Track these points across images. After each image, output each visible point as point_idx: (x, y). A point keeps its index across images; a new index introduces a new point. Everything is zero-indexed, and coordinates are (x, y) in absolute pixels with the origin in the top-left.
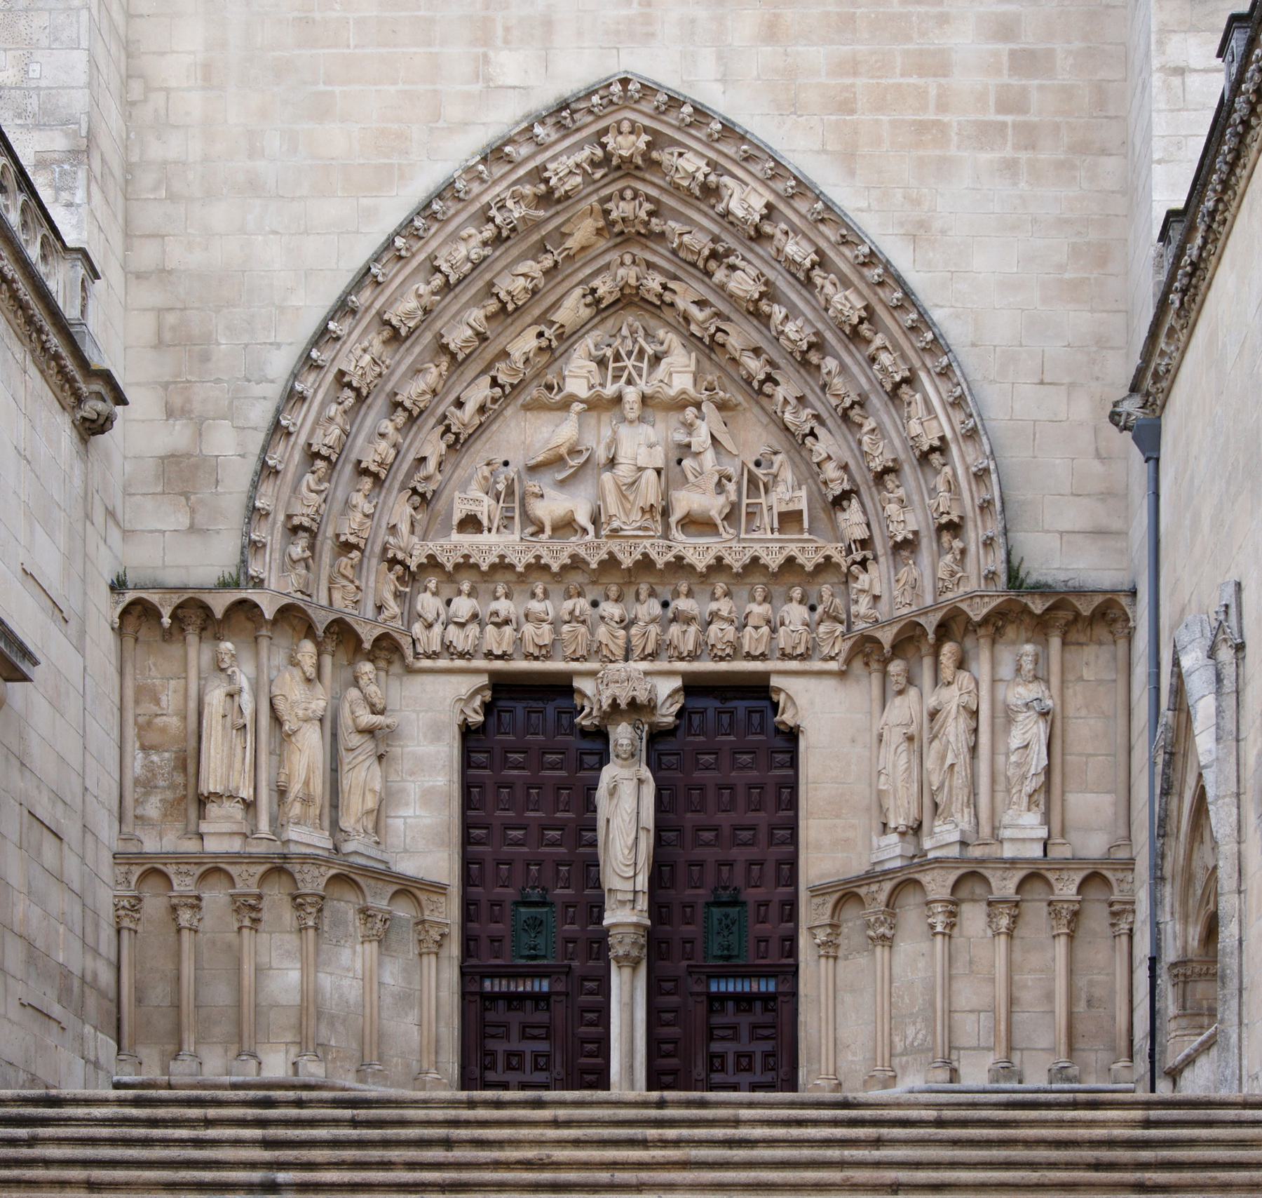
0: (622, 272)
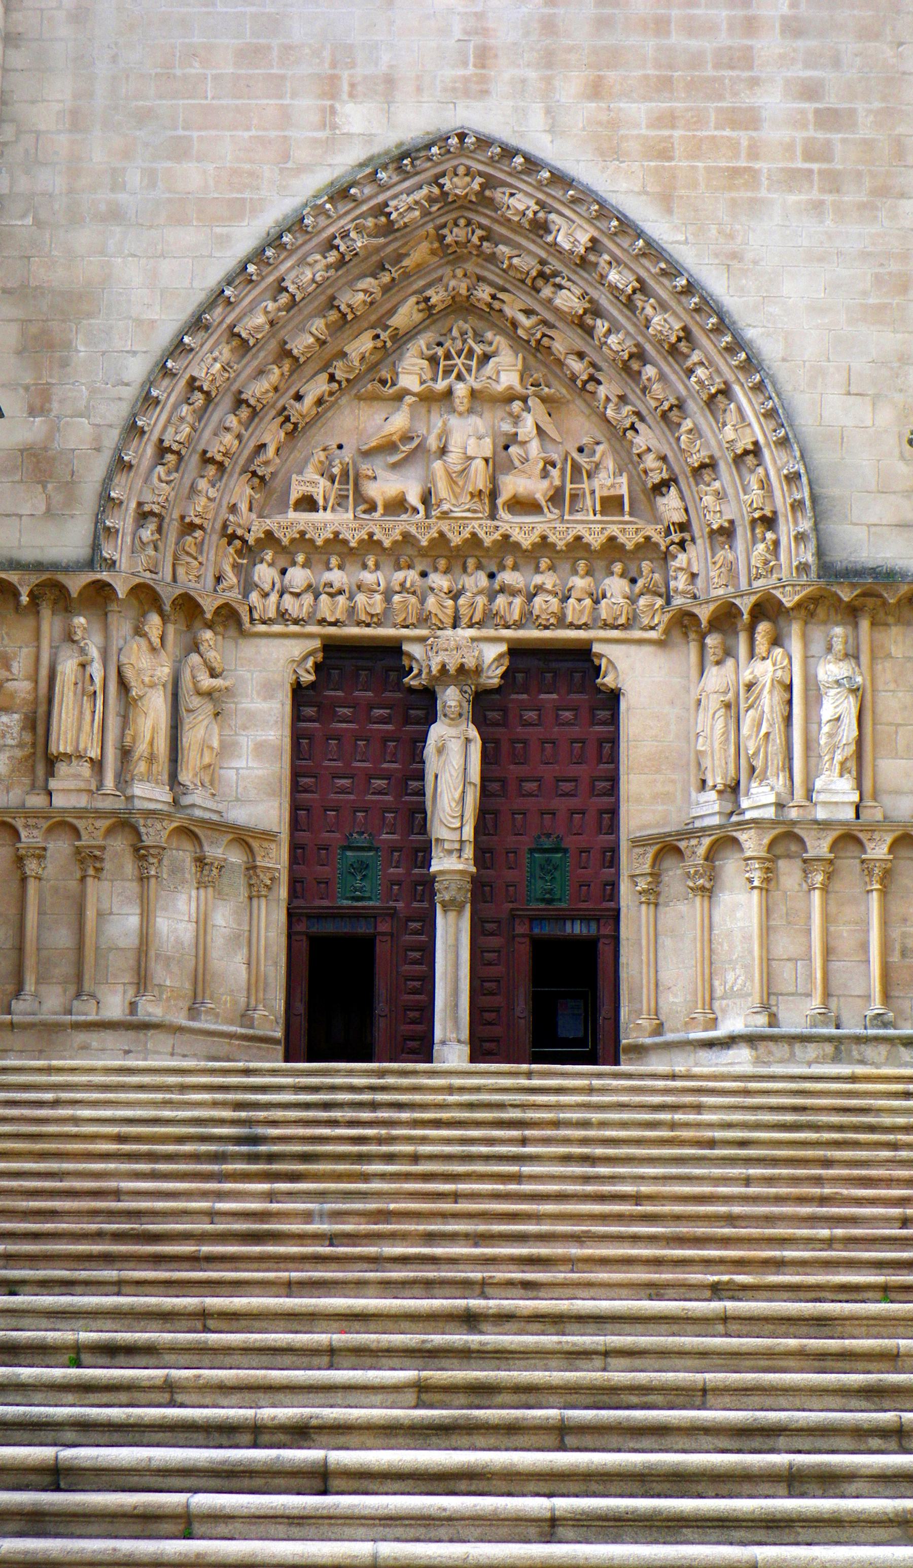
0: (453, 283)
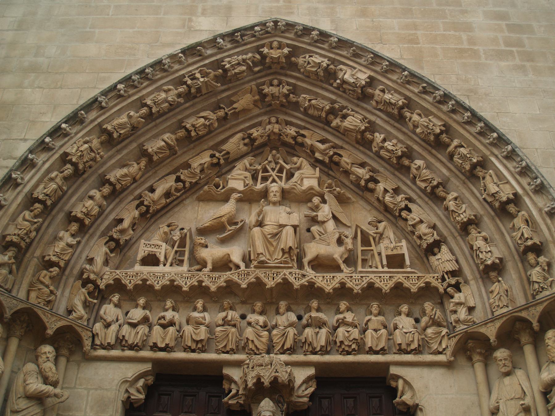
0: (269, 127)
